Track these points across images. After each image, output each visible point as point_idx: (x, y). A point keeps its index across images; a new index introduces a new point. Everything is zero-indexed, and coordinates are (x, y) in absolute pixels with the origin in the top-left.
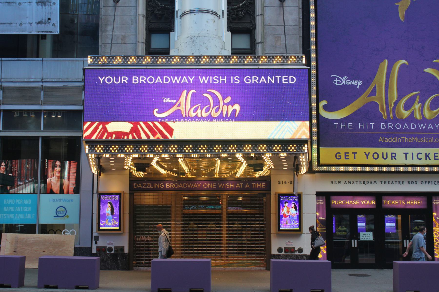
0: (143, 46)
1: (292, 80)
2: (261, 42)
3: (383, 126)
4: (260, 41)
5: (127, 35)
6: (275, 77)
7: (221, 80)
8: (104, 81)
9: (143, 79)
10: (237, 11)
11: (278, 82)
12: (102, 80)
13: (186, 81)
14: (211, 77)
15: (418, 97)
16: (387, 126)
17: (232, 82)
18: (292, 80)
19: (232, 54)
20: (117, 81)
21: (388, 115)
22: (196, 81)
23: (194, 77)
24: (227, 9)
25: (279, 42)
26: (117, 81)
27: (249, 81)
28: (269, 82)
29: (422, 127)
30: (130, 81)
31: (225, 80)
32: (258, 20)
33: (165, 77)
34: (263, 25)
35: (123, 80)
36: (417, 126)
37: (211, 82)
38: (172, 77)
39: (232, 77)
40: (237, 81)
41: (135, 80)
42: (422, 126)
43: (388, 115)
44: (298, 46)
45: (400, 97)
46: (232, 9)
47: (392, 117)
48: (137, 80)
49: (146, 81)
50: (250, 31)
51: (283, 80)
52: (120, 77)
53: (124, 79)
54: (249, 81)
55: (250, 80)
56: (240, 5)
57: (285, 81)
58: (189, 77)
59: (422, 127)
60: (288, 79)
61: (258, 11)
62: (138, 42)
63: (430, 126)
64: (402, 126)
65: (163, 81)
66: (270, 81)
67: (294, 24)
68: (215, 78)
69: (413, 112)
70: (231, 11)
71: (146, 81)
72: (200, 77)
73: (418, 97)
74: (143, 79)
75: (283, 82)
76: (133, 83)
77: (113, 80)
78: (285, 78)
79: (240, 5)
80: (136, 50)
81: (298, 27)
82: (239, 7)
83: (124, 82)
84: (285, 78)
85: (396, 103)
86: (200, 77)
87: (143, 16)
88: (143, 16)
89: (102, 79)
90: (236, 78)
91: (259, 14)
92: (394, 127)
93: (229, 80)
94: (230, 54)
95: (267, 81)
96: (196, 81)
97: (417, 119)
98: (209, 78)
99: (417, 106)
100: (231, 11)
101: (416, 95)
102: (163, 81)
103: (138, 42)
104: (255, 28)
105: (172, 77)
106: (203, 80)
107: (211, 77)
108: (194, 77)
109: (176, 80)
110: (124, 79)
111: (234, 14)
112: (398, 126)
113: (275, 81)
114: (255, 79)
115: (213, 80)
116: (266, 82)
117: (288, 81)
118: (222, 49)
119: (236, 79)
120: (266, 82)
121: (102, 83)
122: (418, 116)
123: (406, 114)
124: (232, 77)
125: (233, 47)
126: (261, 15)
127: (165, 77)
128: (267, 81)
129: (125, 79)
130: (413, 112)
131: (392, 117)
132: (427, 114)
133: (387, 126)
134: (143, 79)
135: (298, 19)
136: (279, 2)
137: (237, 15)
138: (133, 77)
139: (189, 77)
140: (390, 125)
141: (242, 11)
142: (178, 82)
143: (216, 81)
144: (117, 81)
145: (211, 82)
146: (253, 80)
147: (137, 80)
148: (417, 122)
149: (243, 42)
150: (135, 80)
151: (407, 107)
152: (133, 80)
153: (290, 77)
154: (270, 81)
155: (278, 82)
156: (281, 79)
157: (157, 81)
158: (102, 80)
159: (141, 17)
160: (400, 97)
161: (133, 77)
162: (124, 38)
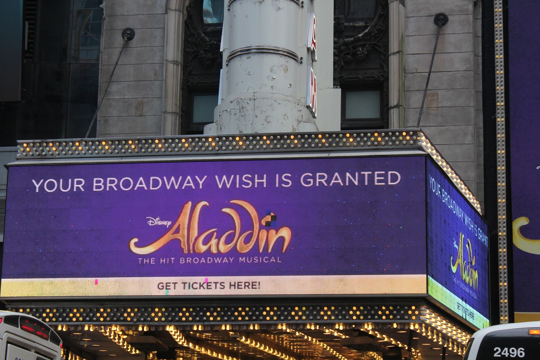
1: (394, 178)
3: (182, 261)
6: (359, 174)
7: (256, 181)
8: (42, 187)
9: (112, 183)
11: (366, 184)
12: (37, 186)
13: (192, 184)
14: (238, 176)
15: (215, 234)
16: (186, 261)
17: (277, 186)
18: (394, 178)
20: (65, 186)
21: (189, 250)
22: (210, 184)
23: (206, 177)
26: (65, 186)
27: (310, 182)
28: (347, 184)
29: (218, 262)
30: (89, 186)
31: (264, 181)
33: (152, 178)
35: (75, 186)
36: (214, 260)
37: (238, 186)
38: (165, 178)
39: (277, 175)
40: (287, 183)
41: (99, 184)
42: (218, 260)
43: (189, 250)
45: (200, 234)
47: (192, 252)
48: (100, 184)
49: (118, 186)
51: (376, 178)
52: (70, 180)
53: (78, 184)
54: (310, 182)
55: (312, 180)
57: (379, 181)
58: (197, 177)
59: (218, 262)
60: (386, 175)
63: (225, 260)
64: (200, 261)
65: (148, 185)
66: (350, 180)
68: (246, 178)
69: (210, 246)
71: (118, 186)
72: (216, 177)
73: (215, 234)
74: (112, 183)
75: (376, 184)
76: (95, 190)
77: (58, 185)
78: (379, 175)
83: (78, 188)
84: (379, 175)
85: (196, 239)
86: (216, 177)
89: (38, 184)
90: (286, 177)
92: (192, 261)
93: (270, 181)
95: (344, 181)
96: (210, 184)
97: (213, 253)
98: (235, 178)
99: (214, 241)
101: (213, 232)
102: (148, 185)
105: (165, 178)
106: (223, 182)
107: (238, 176)
108: (206, 177)
109: (172, 183)
110: (78, 184)
112: (196, 260)
113: (359, 181)
114: (322, 177)
115: (241, 182)
116: (342, 184)
117: (386, 181)
118: (299, 122)
119: (285, 180)
120: (342, 184)
121: (37, 191)
122: (214, 250)
123: (203, 248)
124: (277, 175)
127: (152, 178)
128: (344, 181)
129: (79, 183)
130: (210, 246)
131: (192, 252)
132: (223, 248)
133: (186, 261)
134: (112, 182)
138: (95, 179)
139: (197, 177)
140: (189, 260)
142: (176, 187)
143: (248, 184)
144: (65, 187)
145: (238, 186)
146: (318, 180)
147: (100, 184)
148: (214, 256)
150: (99, 184)
151: (205, 242)
152: (95, 184)
153: (390, 173)
154: (350, 180)
155: (366, 184)
156: (371, 177)
157: (138, 185)
158: (37, 186)
160: (200, 234)
161: (95, 179)
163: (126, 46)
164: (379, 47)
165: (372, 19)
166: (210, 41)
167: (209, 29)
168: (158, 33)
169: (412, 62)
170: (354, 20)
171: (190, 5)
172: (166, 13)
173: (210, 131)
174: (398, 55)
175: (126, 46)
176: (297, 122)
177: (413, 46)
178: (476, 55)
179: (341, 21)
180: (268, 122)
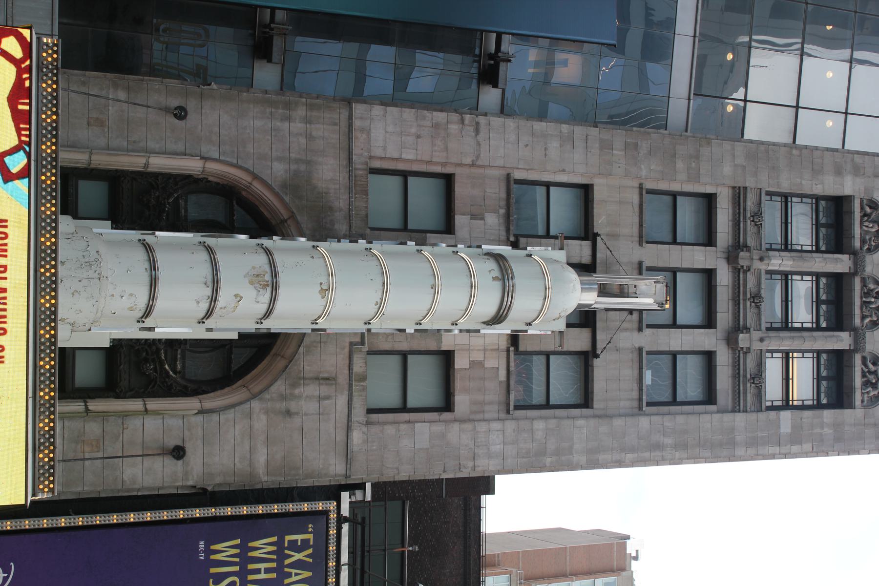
0: (83, 163)
2: (87, 410)
4: (90, 408)
5: (106, 130)
10: (153, 361)
19: (63, 350)
24: (160, 340)
25: (86, 449)
32: (136, 405)
34: (125, 415)
44: (79, 489)
46: (158, 351)
50: (111, 387)
56: (167, 367)
61: (154, 404)
62: (91, 153)
67: (125, 478)
70: (154, 348)
79: (167, 367)
80: (73, 146)
81: (120, 487)
82: (162, 365)
87: (147, 165)
88: (147, 165)
91: (148, 407)
94: (61, 344)
100: (154, 348)
103: (91, 153)
104: (118, 397)
111: (147, 354)
125: (77, 352)
126: (146, 410)
135: (137, 486)
136: (172, 447)
137: (146, 360)
141: (155, 370)
149: (86, 373)
159: (143, 161)
162: (101, 123)
163: (167, 110)
164: (154, 386)
165: (183, 377)
166: (169, 204)
167: (182, 203)
168: (180, 147)
169: (137, 422)
170: (183, 357)
171: (209, 181)
172: (202, 158)
173: (66, 223)
174: (143, 409)
175: (167, 110)
176: (72, 322)
177: (152, 424)
178: (138, 490)
179: (182, 347)
180: (73, 294)
